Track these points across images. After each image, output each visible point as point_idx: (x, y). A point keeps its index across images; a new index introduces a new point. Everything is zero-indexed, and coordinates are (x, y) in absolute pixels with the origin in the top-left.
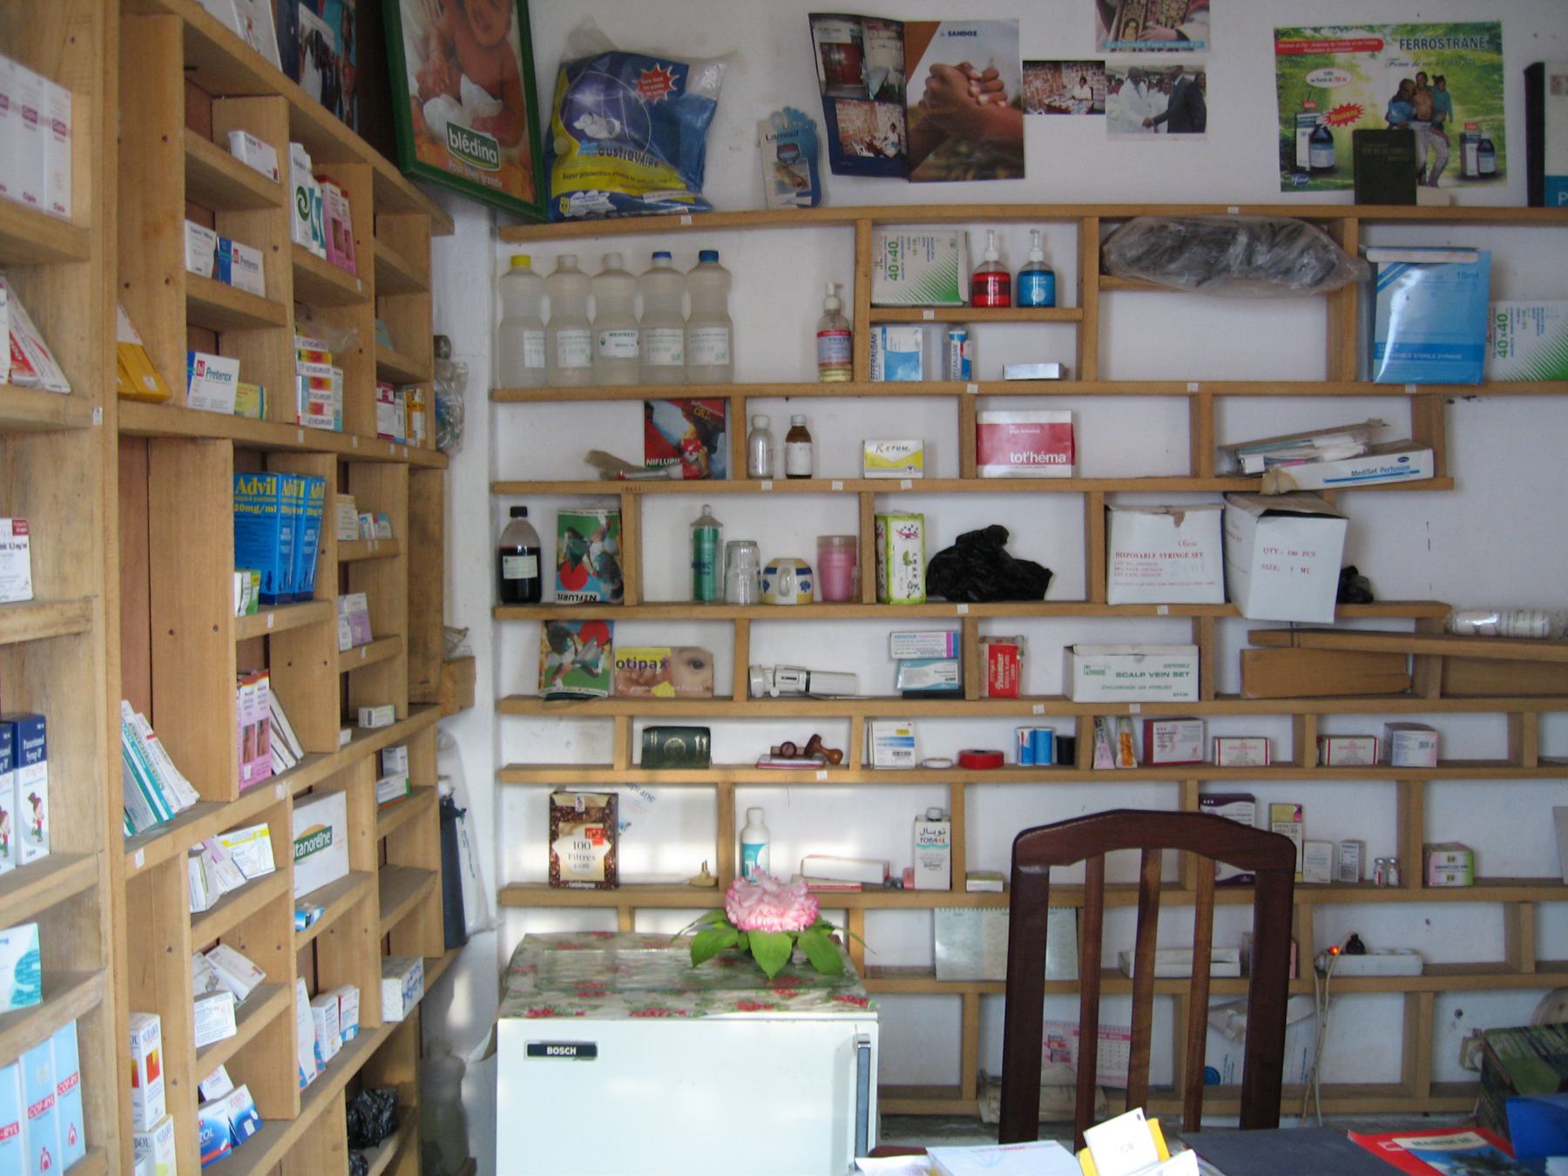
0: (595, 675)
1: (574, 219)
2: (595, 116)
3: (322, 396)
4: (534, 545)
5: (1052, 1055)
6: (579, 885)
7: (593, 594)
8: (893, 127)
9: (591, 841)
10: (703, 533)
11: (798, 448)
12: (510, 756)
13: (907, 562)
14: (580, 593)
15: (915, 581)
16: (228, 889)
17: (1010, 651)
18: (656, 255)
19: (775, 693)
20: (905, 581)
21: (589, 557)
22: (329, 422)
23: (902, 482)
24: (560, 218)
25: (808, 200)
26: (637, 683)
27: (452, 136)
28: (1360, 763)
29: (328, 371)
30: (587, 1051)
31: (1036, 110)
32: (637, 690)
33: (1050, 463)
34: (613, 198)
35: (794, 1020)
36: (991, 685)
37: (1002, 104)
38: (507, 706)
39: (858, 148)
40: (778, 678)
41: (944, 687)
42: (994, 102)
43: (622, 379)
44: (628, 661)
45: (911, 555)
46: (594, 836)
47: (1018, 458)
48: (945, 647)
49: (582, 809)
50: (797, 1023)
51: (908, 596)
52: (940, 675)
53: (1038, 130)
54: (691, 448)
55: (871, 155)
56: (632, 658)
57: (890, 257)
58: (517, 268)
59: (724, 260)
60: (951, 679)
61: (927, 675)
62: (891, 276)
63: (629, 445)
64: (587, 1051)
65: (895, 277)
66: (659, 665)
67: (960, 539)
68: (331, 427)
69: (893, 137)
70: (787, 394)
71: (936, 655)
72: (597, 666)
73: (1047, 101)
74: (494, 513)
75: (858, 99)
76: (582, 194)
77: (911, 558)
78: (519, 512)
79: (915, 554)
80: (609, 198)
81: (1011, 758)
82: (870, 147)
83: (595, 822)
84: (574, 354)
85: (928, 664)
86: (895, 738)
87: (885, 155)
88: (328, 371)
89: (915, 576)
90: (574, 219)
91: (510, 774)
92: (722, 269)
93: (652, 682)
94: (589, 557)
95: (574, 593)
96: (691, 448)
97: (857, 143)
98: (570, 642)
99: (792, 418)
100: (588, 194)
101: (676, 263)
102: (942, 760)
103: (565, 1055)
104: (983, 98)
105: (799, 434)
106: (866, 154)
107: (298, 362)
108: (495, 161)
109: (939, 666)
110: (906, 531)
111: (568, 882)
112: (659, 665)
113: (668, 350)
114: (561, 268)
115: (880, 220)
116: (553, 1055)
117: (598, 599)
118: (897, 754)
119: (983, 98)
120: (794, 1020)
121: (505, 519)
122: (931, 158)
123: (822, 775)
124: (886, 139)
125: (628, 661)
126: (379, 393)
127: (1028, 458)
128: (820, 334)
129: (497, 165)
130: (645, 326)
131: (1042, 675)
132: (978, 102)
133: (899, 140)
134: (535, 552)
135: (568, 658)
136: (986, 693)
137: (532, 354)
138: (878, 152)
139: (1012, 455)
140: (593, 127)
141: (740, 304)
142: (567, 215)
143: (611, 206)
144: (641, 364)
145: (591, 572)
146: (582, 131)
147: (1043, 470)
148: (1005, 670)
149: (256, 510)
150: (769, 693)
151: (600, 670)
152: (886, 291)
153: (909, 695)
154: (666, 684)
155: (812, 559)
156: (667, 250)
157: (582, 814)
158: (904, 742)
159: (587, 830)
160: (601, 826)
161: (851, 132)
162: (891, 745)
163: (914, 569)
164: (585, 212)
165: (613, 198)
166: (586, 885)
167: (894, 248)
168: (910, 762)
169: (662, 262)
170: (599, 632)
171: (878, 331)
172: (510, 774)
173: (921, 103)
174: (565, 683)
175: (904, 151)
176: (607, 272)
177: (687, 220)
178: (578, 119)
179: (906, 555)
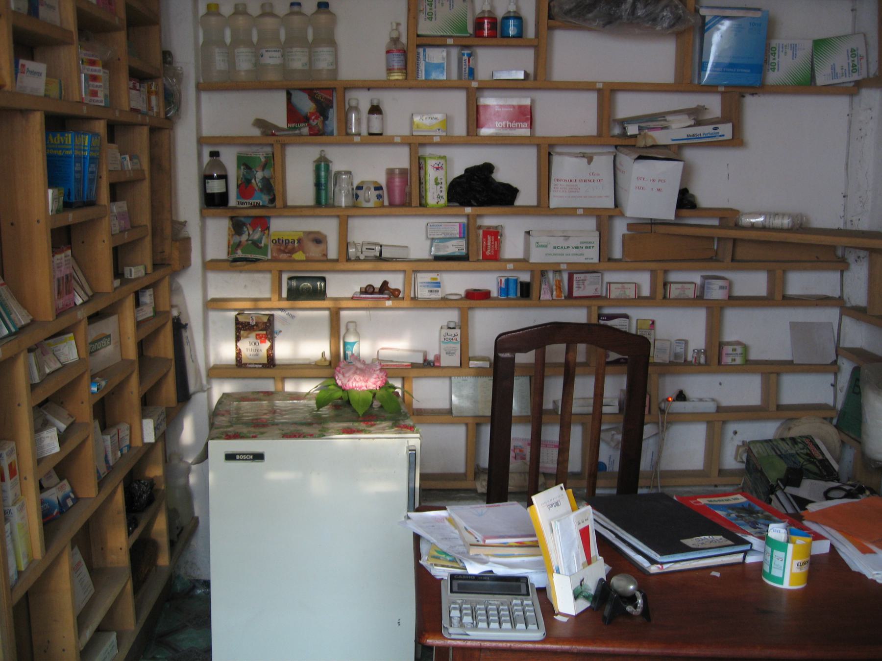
3: (97, 86)
4: (223, 173)
5: (516, 456)
7: (258, 201)
9: (259, 341)
10: (321, 166)
11: (375, 117)
12: (212, 294)
13: (437, 184)
15: (441, 194)
17: (495, 234)
19: (362, 257)
20: (436, 194)
21: (255, 180)
22: (101, 101)
26: (284, 252)
28: (628, 298)
29: (100, 71)
32: (284, 256)
33: (518, 128)
35: (374, 438)
36: (484, 254)
38: (211, 265)
40: (364, 249)
41: (457, 254)
43: (272, 76)
44: (279, 239)
45: (439, 179)
46: (261, 338)
47: (500, 125)
48: (458, 231)
49: (254, 323)
50: (375, 440)
51: (437, 203)
52: (454, 247)
54: (313, 117)
56: (280, 238)
60: (461, 250)
61: (448, 247)
63: (279, 117)
66: (296, 242)
67: (467, 170)
68: (103, 104)
70: (369, 86)
71: (453, 236)
72: (261, 243)
81: (494, 294)
84: (244, 64)
85: (447, 241)
88: (100, 71)
89: (441, 191)
93: (292, 251)
94: (255, 180)
95: (247, 201)
96: (313, 117)
103: (246, 460)
109: (454, 242)
110: (437, 166)
111: (246, 364)
112: (296, 242)
113: (298, 61)
116: (240, 460)
117: (261, 204)
118: (430, 291)
120: (374, 438)
121: (206, 158)
123: (389, 303)
125: (279, 239)
126: (131, 84)
127: (506, 125)
134: (224, 177)
135: (244, 238)
136: (481, 258)
139: (497, 123)
144: (283, 67)
149: (60, 153)
151: (262, 245)
153: (438, 258)
157: (254, 326)
160: (264, 332)
162: (428, 286)
163: (441, 188)
166: (257, 366)
170: (262, 223)
174: (243, 252)
179: (436, 180)
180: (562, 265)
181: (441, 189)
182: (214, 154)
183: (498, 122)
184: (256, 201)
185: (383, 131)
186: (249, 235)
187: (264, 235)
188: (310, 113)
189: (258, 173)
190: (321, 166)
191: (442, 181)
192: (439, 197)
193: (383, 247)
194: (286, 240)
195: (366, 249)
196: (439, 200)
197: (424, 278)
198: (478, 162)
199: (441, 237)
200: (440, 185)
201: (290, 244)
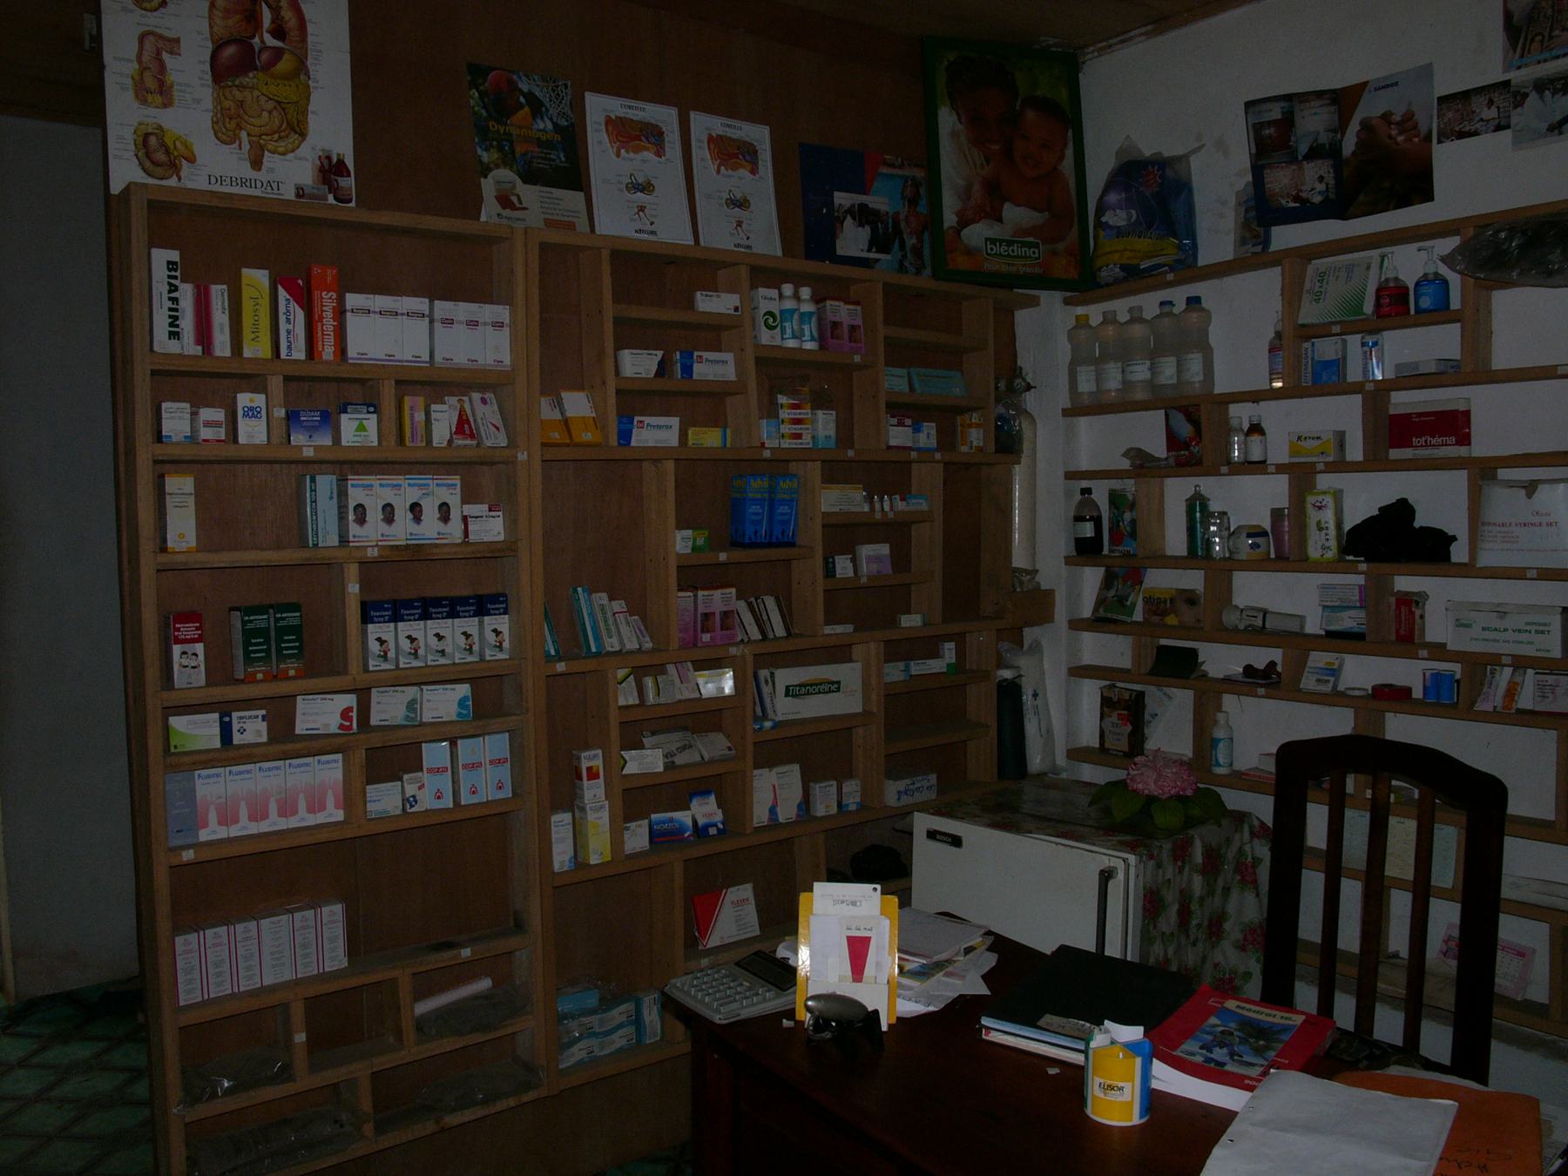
0: (1124, 606)
1: (1107, 285)
2: (1118, 211)
3: (801, 429)
4: (1095, 514)
5: (1447, 951)
6: (1115, 753)
7: (1129, 549)
8: (1321, 179)
9: (1120, 722)
10: (1197, 506)
11: (1256, 438)
12: (1088, 659)
13: (1320, 529)
14: (1121, 548)
15: (1327, 544)
16: (683, 698)
17: (1410, 603)
18: (1162, 304)
19: (1241, 627)
20: (1323, 544)
21: (1123, 523)
22: (809, 443)
23: (1317, 465)
24: (1100, 286)
25: (1259, 249)
26: (1156, 614)
27: (989, 247)
29: (807, 413)
30: (956, 841)
31: (1448, 139)
32: (1156, 619)
33: (1443, 445)
34: (1123, 268)
35: (1072, 847)
36: (1397, 631)
37: (1416, 140)
38: (1076, 625)
39: (1284, 202)
40: (1244, 616)
41: (1356, 630)
42: (1409, 140)
43: (1140, 395)
44: (1150, 597)
45: (1323, 522)
46: (1122, 719)
47: (1419, 442)
48: (1357, 598)
49: (1115, 700)
50: (1074, 850)
51: (1322, 556)
52: (1349, 621)
53: (1448, 160)
54: (1193, 443)
55: (1298, 205)
56: (1152, 595)
57: (1318, 284)
58: (1082, 323)
59: (1204, 304)
60: (1362, 624)
61: (1342, 619)
62: (1315, 300)
63: (1157, 446)
64: (956, 841)
65: (1317, 301)
66: (1168, 602)
67: (1380, 509)
68: (811, 446)
69: (1321, 187)
70: (1255, 397)
71: (1350, 605)
72: (1127, 601)
73: (1457, 129)
74: (1068, 494)
75: (1286, 162)
76: (1105, 268)
77: (1323, 525)
78: (1086, 491)
79: (1326, 522)
80: (1120, 268)
81: (1418, 693)
82: (1297, 199)
83: (1123, 709)
84: (1113, 379)
85: (1342, 611)
86: (1321, 668)
87: (1313, 203)
88: (807, 413)
89: (1328, 540)
90: (1107, 285)
91: (1081, 671)
92: (1203, 310)
93: (1164, 613)
94: (1123, 523)
95: (1117, 548)
96: (1193, 443)
97: (1282, 197)
98: (1116, 583)
99: (1250, 417)
100: (1109, 267)
101: (1176, 310)
102: (1359, 689)
103: (945, 842)
104: (1400, 138)
105: (1256, 429)
106: (1292, 205)
107: (780, 411)
108: (1037, 255)
109: (1352, 613)
110: (1318, 504)
111: (1109, 749)
112: (1168, 602)
113: (1168, 371)
114: (1109, 319)
115: (1308, 253)
116: (939, 840)
117: (1131, 553)
118: (1318, 681)
119: (1400, 138)
120: (1072, 847)
121: (1078, 497)
122: (1361, 197)
123: (1261, 691)
124: (1312, 189)
125: (1150, 597)
126: (894, 421)
127: (1426, 441)
128: (1270, 351)
129: (1039, 258)
130: (1154, 354)
131: (1437, 627)
132: (1397, 144)
133: (1327, 188)
134: (1097, 522)
135: (1112, 593)
136: (1393, 638)
137: (1086, 384)
138: (1303, 201)
139: (1414, 439)
140: (1116, 218)
141: (1216, 335)
142: (1102, 283)
143: (1123, 274)
144: (1151, 384)
145: (1126, 533)
146: (1106, 223)
147: (1437, 451)
148: (1406, 620)
149: (739, 496)
150: (1237, 626)
151: (1128, 603)
152: (1309, 314)
153: (1330, 635)
154: (1172, 615)
155: (1267, 524)
156: (1169, 299)
157: (1116, 703)
158: (1329, 672)
159: (1119, 715)
160: (1126, 712)
161: (1277, 190)
162: (1317, 673)
163: (1326, 534)
164: (1112, 280)
165: (1123, 268)
166: (1119, 753)
167: (1322, 277)
168: (1327, 688)
169: (1166, 309)
170: (1136, 577)
171: (1307, 345)
172: (1081, 671)
173: (1354, 153)
174: (1105, 611)
175: (1332, 196)
176: (1132, 321)
177: (1170, 277)
178: (1104, 215)
179: (1319, 523)
180: (1426, 656)
181: (1328, 537)
182: (1086, 491)
183: (1417, 438)
184: (1125, 548)
185: (1266, 456)
186: (1117, 591)
187: (1133, 591)
188: (1189, 437)
189: (1126, 514)
190: (1197, 506)
191: (1327, 525)
192: (1324, 548)
193: (1267, 615)
194: (1158, 599)
195: (1248, 616)
196: (1325, 552)
197: (1318, 659)
198: (1389, 499)
199: (1336, 604)
200: (1324, 531)
201: (1162, 604)
